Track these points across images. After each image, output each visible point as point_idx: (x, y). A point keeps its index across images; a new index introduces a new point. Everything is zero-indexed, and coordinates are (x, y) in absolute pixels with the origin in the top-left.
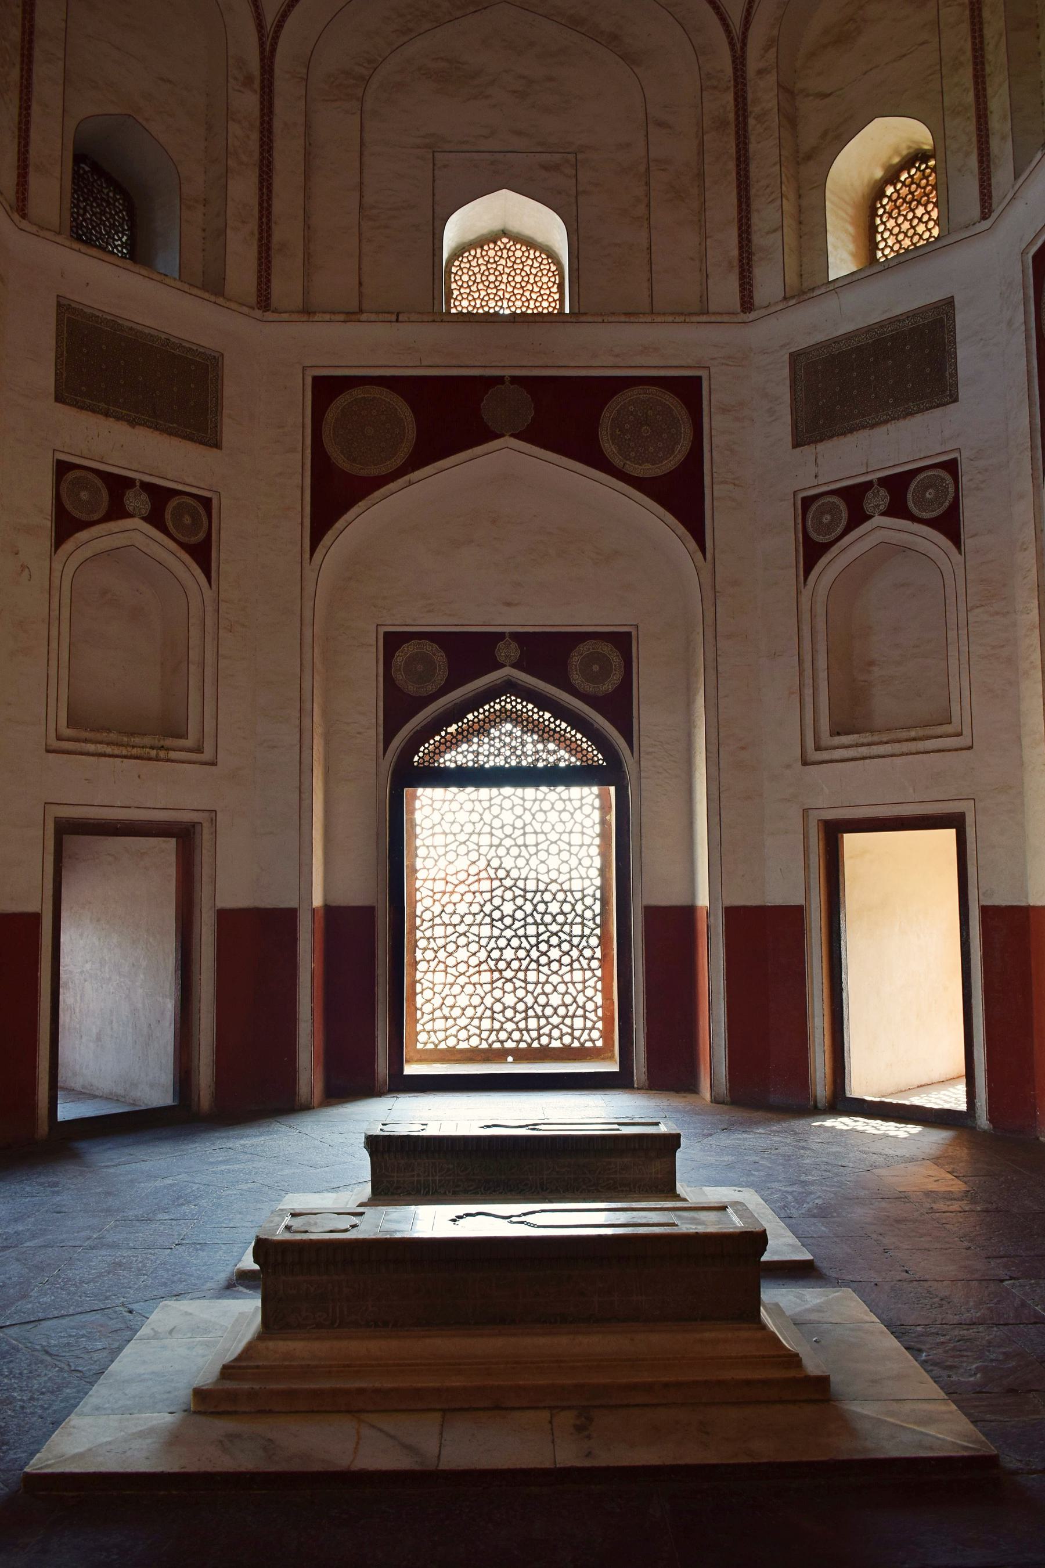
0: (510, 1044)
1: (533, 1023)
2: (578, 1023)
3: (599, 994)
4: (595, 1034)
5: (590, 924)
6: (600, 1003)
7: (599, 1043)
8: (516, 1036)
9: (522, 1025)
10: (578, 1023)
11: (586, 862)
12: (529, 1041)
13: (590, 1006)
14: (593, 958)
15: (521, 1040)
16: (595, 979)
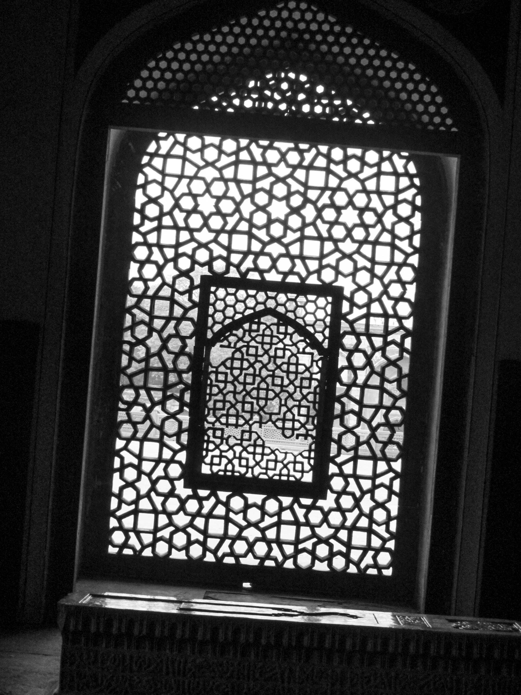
0: (250, 561)
1: (288, 533)
2: (359, 539)
3: (395, 499)
4: (384, 558)
5: (392, 387)
6: (394, 512)
7: (388, 572)
8: (261, 549)
9: (271, 534)
10: (359, 539)
11: (395, 290)
12: (280, 558)
13: (380, 515)
14: (390, 441)
15: (268, 556)
16: (391, 475)
